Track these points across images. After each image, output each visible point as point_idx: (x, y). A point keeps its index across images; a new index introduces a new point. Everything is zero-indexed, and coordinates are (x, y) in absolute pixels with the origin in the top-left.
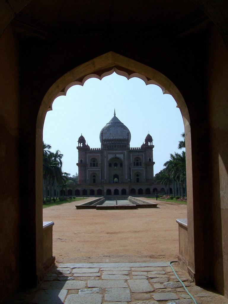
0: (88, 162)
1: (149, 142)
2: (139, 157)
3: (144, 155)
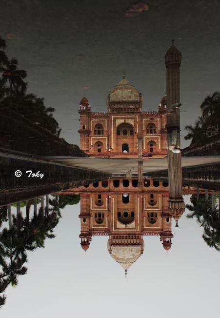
0: (160, 219)
2: (98, 224)
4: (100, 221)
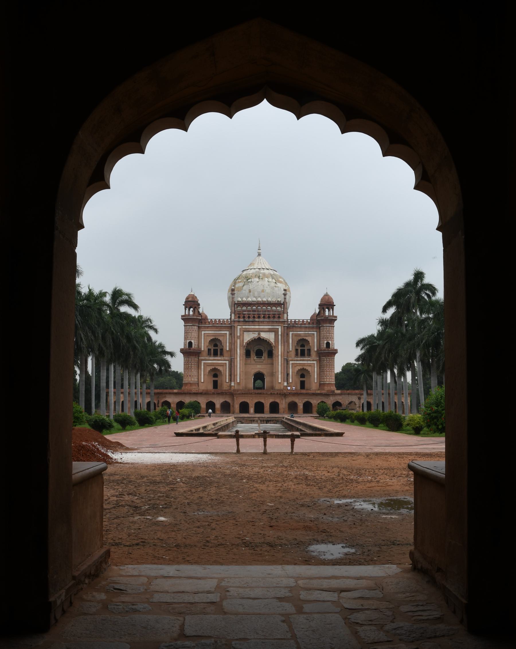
0: (203, 347)
1: (327, 310)
3: (315, 335)
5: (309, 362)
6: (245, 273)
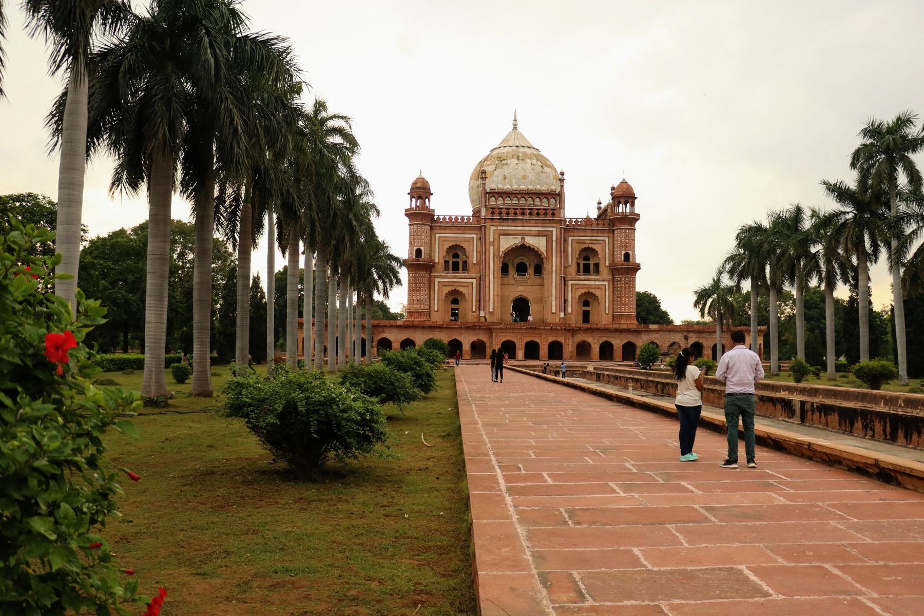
0: (438, 257)
2: (594, 247)
3: (607, 242)
4: (587, 253)
5: (597, 283)
6: (495, 152)
